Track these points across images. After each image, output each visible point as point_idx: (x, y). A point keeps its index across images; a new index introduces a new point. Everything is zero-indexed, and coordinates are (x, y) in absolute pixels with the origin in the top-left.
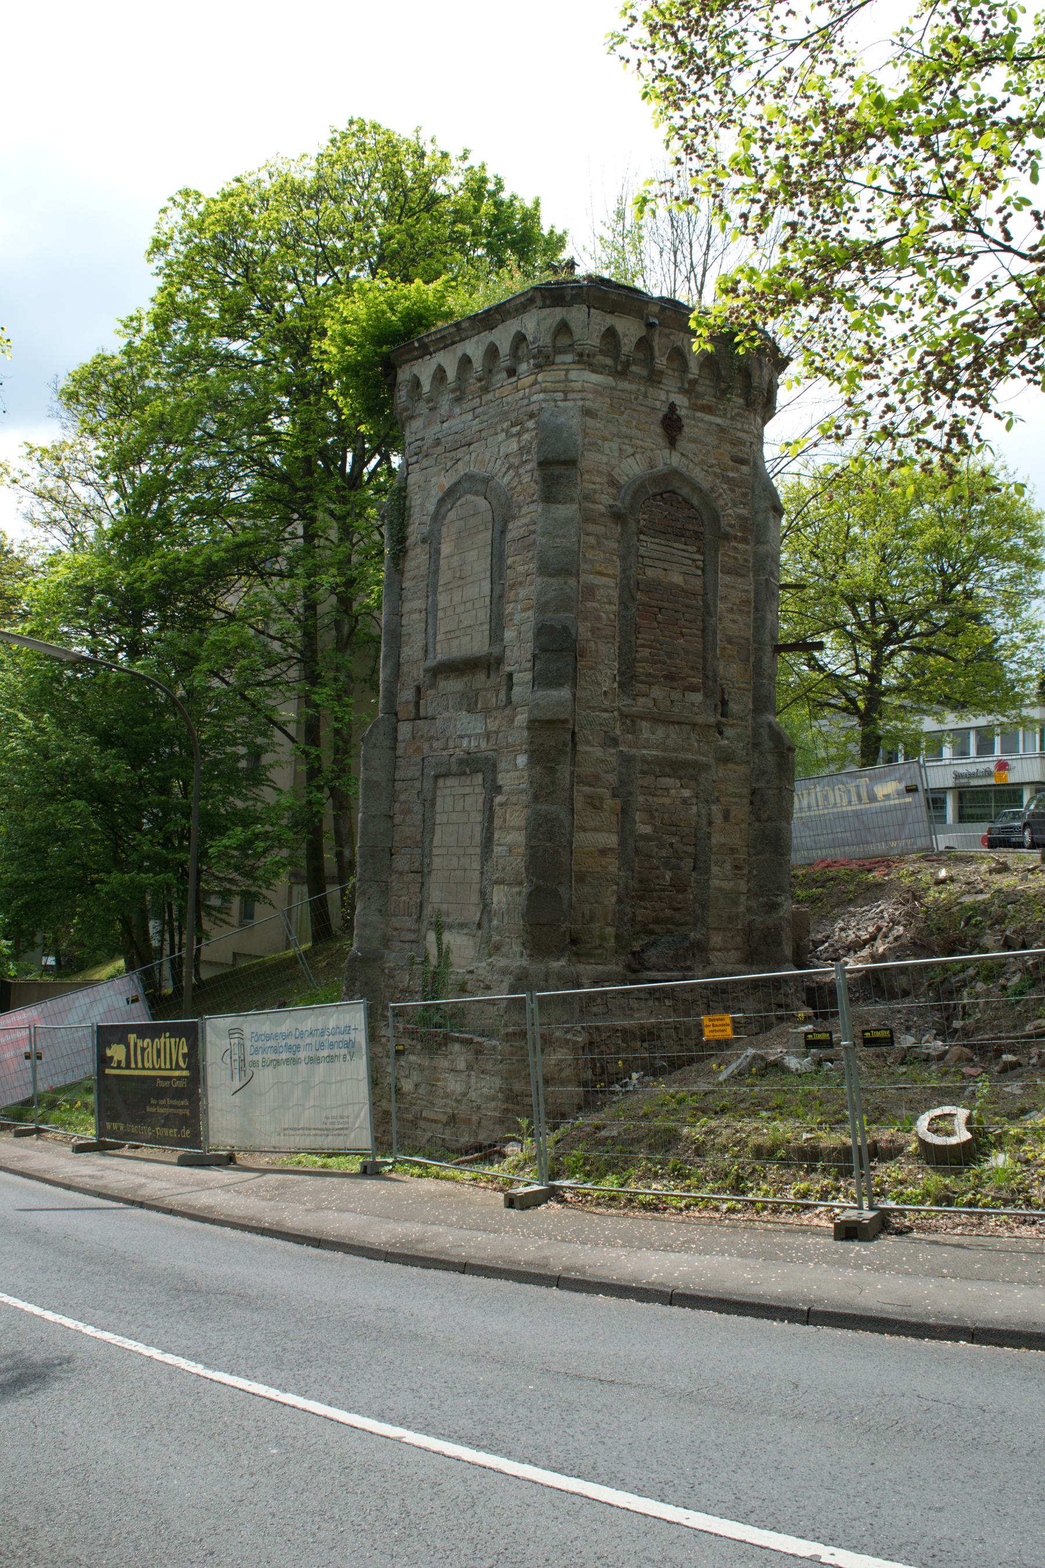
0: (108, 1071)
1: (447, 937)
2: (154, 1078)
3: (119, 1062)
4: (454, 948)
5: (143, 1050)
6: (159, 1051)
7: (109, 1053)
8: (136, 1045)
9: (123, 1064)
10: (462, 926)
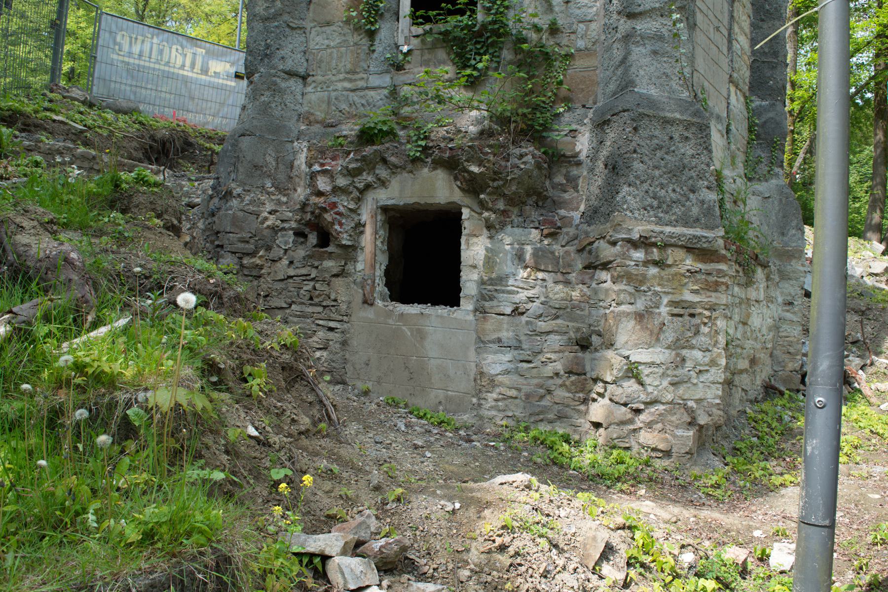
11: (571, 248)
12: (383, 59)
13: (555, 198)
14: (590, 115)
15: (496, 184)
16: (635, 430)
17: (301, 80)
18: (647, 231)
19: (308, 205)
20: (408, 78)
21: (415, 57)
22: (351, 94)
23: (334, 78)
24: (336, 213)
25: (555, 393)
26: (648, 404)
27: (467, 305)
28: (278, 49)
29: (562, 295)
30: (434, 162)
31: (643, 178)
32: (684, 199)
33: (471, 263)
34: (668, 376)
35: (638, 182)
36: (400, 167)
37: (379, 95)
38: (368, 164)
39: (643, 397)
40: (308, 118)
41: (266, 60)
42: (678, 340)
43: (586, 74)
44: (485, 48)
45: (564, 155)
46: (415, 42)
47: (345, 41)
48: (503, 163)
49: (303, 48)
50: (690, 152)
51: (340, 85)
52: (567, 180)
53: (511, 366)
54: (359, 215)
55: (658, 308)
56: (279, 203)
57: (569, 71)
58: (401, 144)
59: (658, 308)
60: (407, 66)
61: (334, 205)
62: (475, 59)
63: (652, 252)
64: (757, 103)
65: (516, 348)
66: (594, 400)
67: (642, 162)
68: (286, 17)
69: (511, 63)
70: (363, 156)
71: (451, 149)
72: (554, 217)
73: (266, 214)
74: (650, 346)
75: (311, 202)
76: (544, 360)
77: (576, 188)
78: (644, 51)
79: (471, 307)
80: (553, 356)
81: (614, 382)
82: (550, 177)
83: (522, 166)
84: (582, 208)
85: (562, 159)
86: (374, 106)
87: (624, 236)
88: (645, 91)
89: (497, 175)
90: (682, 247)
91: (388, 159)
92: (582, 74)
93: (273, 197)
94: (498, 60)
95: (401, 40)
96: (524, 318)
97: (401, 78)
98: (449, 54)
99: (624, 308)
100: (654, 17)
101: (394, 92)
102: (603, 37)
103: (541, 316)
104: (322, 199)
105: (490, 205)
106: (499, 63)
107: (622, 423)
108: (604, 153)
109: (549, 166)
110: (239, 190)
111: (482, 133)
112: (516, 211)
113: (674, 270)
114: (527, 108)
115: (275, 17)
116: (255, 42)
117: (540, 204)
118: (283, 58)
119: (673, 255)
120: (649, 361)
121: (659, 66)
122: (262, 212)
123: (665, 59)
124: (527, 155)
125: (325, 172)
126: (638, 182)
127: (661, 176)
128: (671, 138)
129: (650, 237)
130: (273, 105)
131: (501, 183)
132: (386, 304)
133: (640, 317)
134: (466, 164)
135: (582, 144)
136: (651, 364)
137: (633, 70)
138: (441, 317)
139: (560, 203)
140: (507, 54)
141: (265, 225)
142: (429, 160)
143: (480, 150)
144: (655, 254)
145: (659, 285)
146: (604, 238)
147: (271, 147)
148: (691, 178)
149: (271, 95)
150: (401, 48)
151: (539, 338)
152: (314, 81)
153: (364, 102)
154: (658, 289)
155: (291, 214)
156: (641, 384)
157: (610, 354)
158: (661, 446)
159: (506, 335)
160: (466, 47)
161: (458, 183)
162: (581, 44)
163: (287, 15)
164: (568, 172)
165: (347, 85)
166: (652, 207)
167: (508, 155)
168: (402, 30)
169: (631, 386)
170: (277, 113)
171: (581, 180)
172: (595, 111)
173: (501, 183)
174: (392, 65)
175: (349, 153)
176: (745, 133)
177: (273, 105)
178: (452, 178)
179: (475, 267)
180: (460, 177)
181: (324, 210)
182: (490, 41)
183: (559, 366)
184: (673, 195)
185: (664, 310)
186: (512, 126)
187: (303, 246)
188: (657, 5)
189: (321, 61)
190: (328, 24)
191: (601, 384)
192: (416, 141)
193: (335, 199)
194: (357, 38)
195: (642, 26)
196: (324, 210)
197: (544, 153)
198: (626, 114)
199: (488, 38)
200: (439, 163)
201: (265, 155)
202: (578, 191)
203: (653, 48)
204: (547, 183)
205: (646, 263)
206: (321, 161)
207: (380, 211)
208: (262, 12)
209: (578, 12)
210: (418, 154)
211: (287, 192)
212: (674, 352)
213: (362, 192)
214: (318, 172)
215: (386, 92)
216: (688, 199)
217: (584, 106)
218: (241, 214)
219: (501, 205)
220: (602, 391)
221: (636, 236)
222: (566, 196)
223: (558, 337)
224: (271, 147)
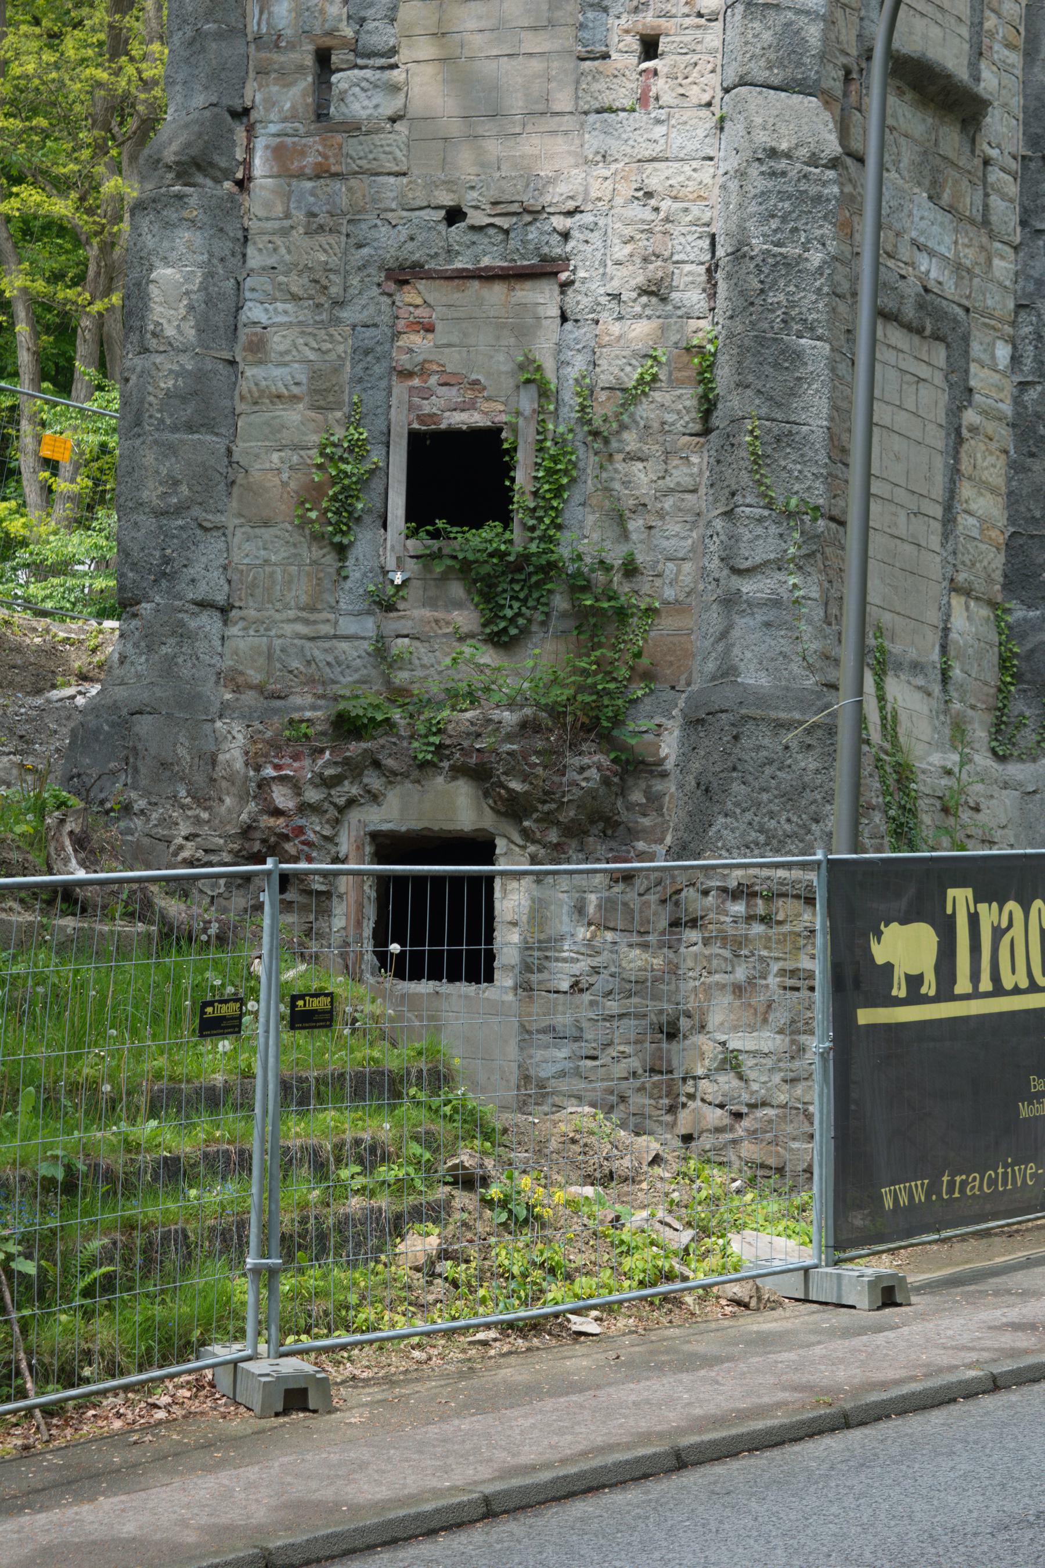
0: (865, 1016)
1: (897, 689)
3: (915, 981)
4: (903, 717)
5: (998, 933)
7: (880, 953)
8: (974, 920)
9: (929, 987)
10: (916, 667)
11: (652, 898)
12: (361, 591)
13: (631, 825)
14: (681, 704)
15: (546, 808)
16: (734, 1142)
17: (218, 614)
18: (749, 877)
19: (256, 828)
20: (405, 626)
21: (414, 592)
22: (308, 644)
23: (278, 616)
24: (303, 843)
25: (631, 1101)
26: (753, 1106)
27: (504, 980)
28: (185, 566)
29: (639, 963)
30: (452, 768)
31: (744, 805)
32: (803, 832)
33: (509, 919)
34: (780, 1070)
35: (738, 811)
36: (401, 774)
37: (356, 649)
38: (353, 769)
39: (746, 1097)
40: (233, 679)
41: (164, 583)
42: (793, 1022)
43: (676, 639)
44: (526, 591)
45: (643, 762)
46: (412, 565)
47: (295, 555)
48: (556, 779)
49: (222, 561)
50: (813, 766)
51: (288, 629)
52: (647, 799)
53: (569, 1065)
54: (337, 844)
55: (765, 978)
56: (198, 821)
57: (652, 634)
58: (401, 738)
59: (765, 978)
60: (401, 605)
61: (300, 830)
62: (511, 607)
63: (756, 905)
64: (1019, 613)
65: (577, 1039)
66: (684, 1105)
67: (744, 783)
68: (196, 511)
69: (564, 615)
70: (346, 758)
71: (478, 750)
72: (629, 852)
73: (180, 841)
74: (752, 1028)
75: (262, 825)
76: (615, 1054)
77: (659, 810)
78: (752, 623)
79: (509, 983)
80: (627, 1049)
81: (707, 1077)
82: (623, 792)
83: (584, 784)
84: (668, 840)
85: (641, 767)
86: (348, 667)
87: (719, 884)
88: (752, 681)
89: (548, 795)
90: (797, 897)
91: (384, 762)
92: (671, 638)
93: (189, 813)
94: (546, 609)
95: (391, 563)
96: (587, 997)
97: (392, 624)
98: (469, 592)
99: (717, 977)
100: (768, 572)
101: (381, 652)
102: (701, 587)
103: (610, 993)
104: (281, 821)
105: (538, 835)
106: (547, 614)
107: (718, 1130)
108: (696, 766)
109: (621, 779)
110: (141, 804)
111: (524, 725)
112: (574, 843)
113: (786, 928)
114: (591, 694)
115: (179, 511)
116: (143, 549)
117: (609, 832)
118: (193, 581)
119: (784, 908)
120: (753, 1048)
121: (773, 643)
122: (174, 837)
123: (782, 633)
124: (589, 767)
125: (283, 779)
126: (738, 811)
127: (770, 801)
128: (787, 748)
129: (753, 885)
130: (180, 660)
131: (554, 806)
132: (381, 980)
133: (738, 990)
134: (503, 778)
135: (669, 747)
136: (755, 1053)
137: (736, 651)
138: (467, 997)
139: (638, 832)
140: (560, 602)
141: (179, 858)
142: (446, 764)
143: (524, 758)
144: (760, 907)
145: (766, 948)
146: (694, 884)
147: (184, 731)
148: (815, 801)
149: (177, 644)
150: (391, 575)
151: (608, 1024)
152: (242, 618)
153: (330, 659)
154: (764, 953)
155: (222, 841)
156: (741, 1077)
157: (700, 1039)
158: (772, 1162)
159: (563, 1020)
160: (496, 585)
161: (491, 802)
162: (669, 593)
163: (197, 507)
164: (649, 787)
165: (301, 629)
166: (757, 844)
167: (565, 766)
168: (393, 547)
169: (727, 1081)
170: (186, 672)
171: (667, 798)
172: (688, 698)
173: (554, 806)
174: (379, 603)
175: (322, 751)
176: (992, 676)
177: (180, 660)
178: (480, 793)
179: (515, 924)
180: (493, 793)
181: (286, 838)
182: (534, 579)
183: (635, 1063)
184: (787, 827)
185: (773, 981)
186: (569, 719)
187: (242, 892)
188: (772, 556)
189: (254, 585)
190: (266, 524)
191: (691, 1082)
192: (426, 736)
193: (302, 822)
194: (316, 553)
195: (748, 587)
196: (286, 838)
197: (613, 761)
198: (723, 716)
199: (530, 574)
200: (459, 771)
201: (175, 745)
202: (662, 815)
203: (765, 618)
204: (619, 803)
205: (750, 918)
206: (276, 761)
207: (368, 839)
208: (156, 502)
209: (665, 543)
210: (429, 757)
211: (208, 803)
212: (787, 1039)
213: (341, 810)
214: (273, 778)
215: (367, 646)
216: (809, 832)
217: (673, 688)
218: (146, 841)
219: (553, 836)
220: (691, 1090)
221: (732, 884)
222: (646, 822)
223: (633, 1022)
224: (184, 731)
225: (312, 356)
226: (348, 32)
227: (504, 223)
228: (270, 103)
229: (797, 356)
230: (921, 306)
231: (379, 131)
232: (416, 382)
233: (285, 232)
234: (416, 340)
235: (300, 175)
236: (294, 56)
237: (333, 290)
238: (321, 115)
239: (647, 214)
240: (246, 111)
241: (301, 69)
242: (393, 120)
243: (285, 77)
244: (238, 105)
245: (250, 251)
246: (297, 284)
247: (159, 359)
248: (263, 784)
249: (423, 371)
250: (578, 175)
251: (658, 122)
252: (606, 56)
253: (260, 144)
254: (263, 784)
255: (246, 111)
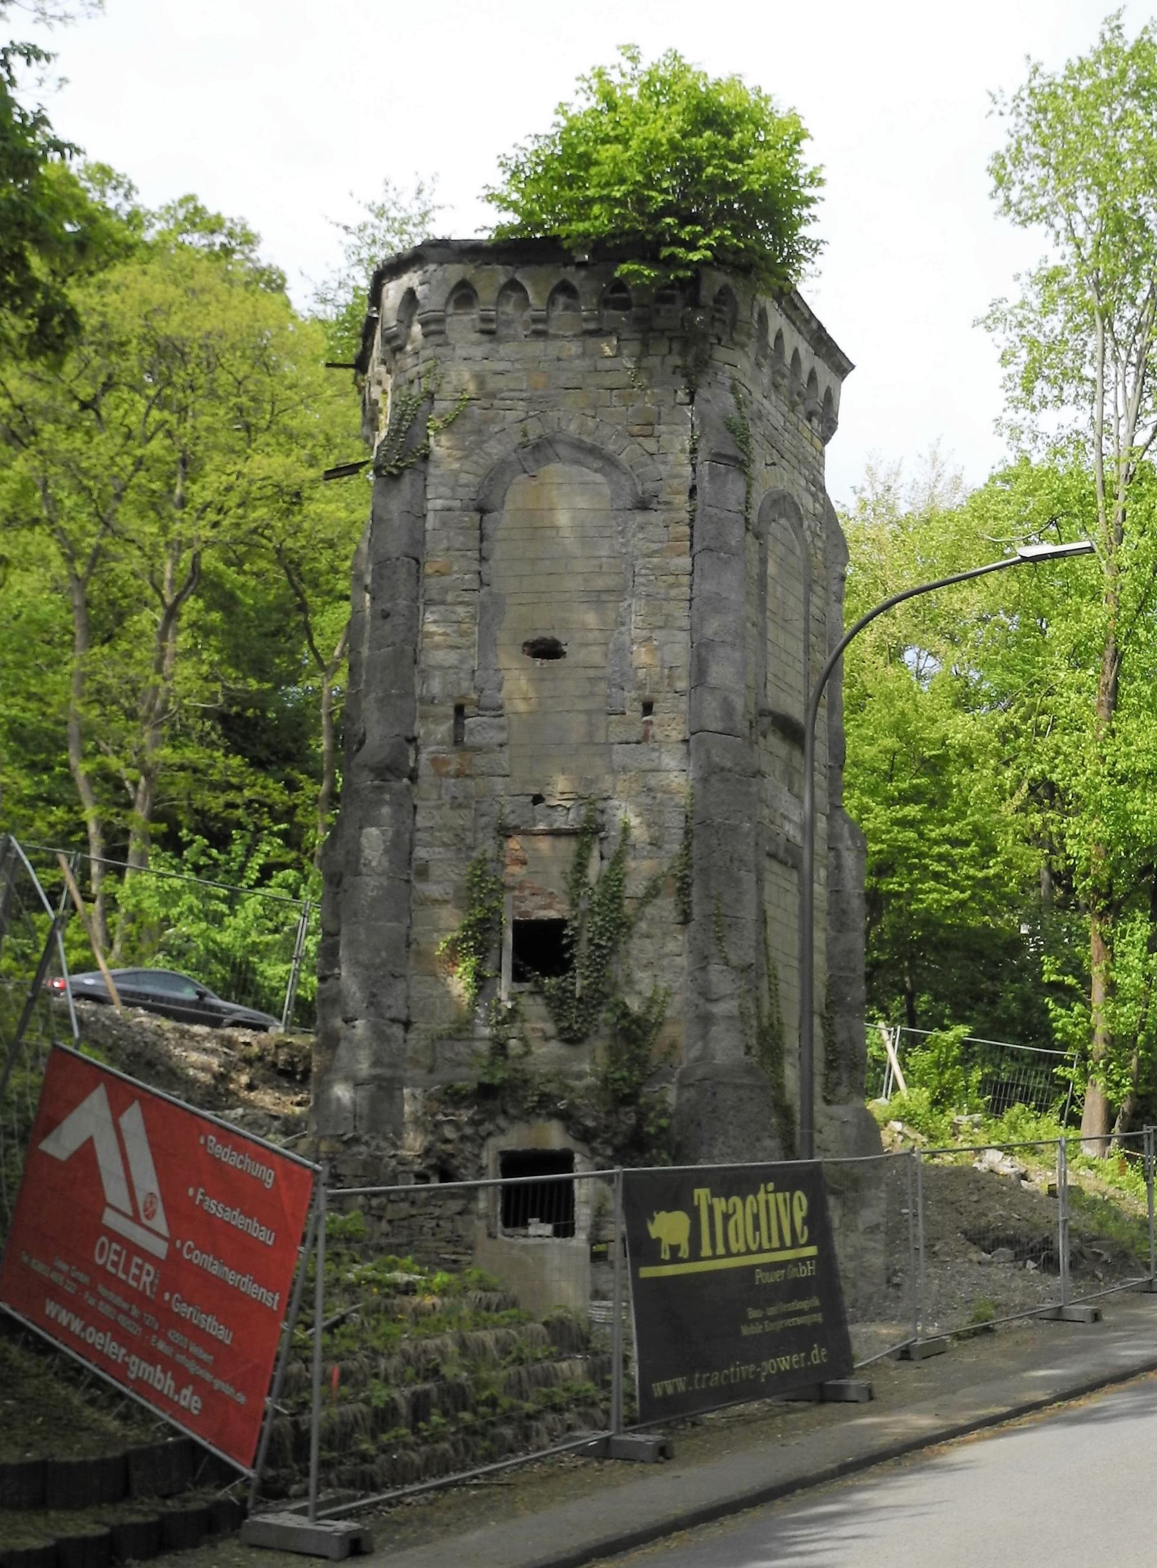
2: (751, 1269)
5: (727, 1217)
6: (756, 1217)
8: (711, 1209)
61: (462, 1151)
110: (366, 1138)
181: (452, 1156)
213: (484, 1139)
225: (456, 878)
226: (474, 696)
227: (568, 804)
228: (428, 733)
229: (738, 881)
230: (787, 850)
231: (493, 751)
232: (517, 893)
233: (439, 807)
234: (516, 869)
235: (447, 775)
236: (442, 709)
237: (469, 841)
238: (458, 741)
239: (649, 801)
240: (415, 739)
241: (446, 717)
242: (501, 745)
243: (437, 719)
244: (410, 735)
245: (418, 818)
246: (447, 837)
247: (367, 879)
248: (437, 1125)
249: (521, 887)
250: (608, 778)
251: (654, 750)
252: (623, 713)
253: (424, 757)
254: (437, 1125)
255: (415, 739)
